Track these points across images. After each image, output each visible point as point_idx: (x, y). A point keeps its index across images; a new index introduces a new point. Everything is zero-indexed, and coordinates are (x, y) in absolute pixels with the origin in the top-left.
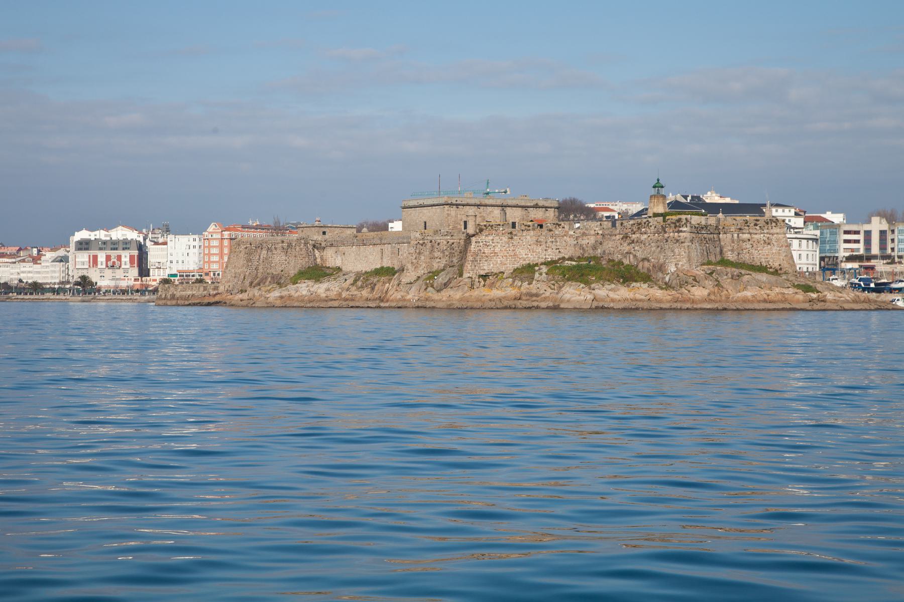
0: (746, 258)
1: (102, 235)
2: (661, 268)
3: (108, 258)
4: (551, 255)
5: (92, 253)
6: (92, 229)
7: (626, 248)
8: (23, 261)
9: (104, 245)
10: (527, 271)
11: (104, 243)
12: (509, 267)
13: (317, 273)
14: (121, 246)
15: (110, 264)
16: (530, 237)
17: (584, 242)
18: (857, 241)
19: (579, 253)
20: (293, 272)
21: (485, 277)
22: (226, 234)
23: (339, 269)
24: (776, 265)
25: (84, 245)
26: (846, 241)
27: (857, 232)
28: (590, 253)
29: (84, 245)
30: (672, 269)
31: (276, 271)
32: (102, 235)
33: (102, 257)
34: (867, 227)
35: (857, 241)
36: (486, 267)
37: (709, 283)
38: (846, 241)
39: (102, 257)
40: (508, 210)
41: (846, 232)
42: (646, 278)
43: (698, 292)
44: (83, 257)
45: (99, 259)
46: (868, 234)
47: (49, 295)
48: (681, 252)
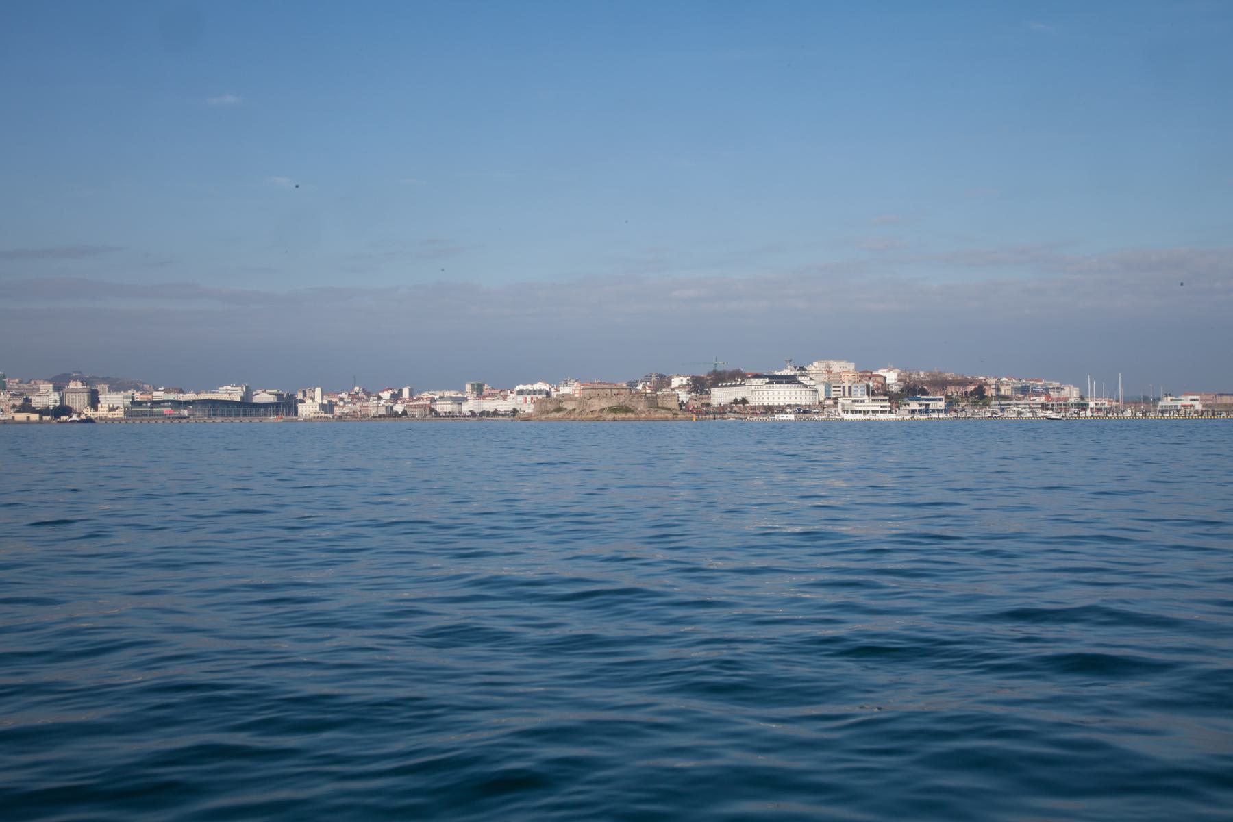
0: (665, 406)
1: (529, 387)
2: (637, 409)
3: (532, 399)
4: (610, 405)
5: (524, 396)
6: (525, 384)
7: (630, 403)
8: (498, 399)
9: (529, 392)
10: (602, 410)
11: (530, 391)
12: (599, 408)
13: (559, 410)
14: (538, 393)
15: (533, 401)
16: (605, 400)
17: (620, 401)
18: (840, 391)
19: (618, 404)
20: (552, 410)
21: (592, 412)
22: (582, 387)
23: (566, 409)
24: (673, 407)
25: (521, 392)
26: (834, 391)
27: (840, 387)
28: (621, 404)
29: (521, 392)
30: (639, 409)
31: (547, 409)
32: (529, 387)
33: (529, 398)
34: (843, 384)
35: (840, 391)
36: (592, 409)
37: (647, 413)
38: (834, 391)
39: (529, 398)
40: (613, 390)
41: (834, 387)
42: (632, 412)
43: (643, 415)
44: (520, 398)
45: (528, 399)
46: (844, 387)
47: (500, 418)
48: (642, 404)
